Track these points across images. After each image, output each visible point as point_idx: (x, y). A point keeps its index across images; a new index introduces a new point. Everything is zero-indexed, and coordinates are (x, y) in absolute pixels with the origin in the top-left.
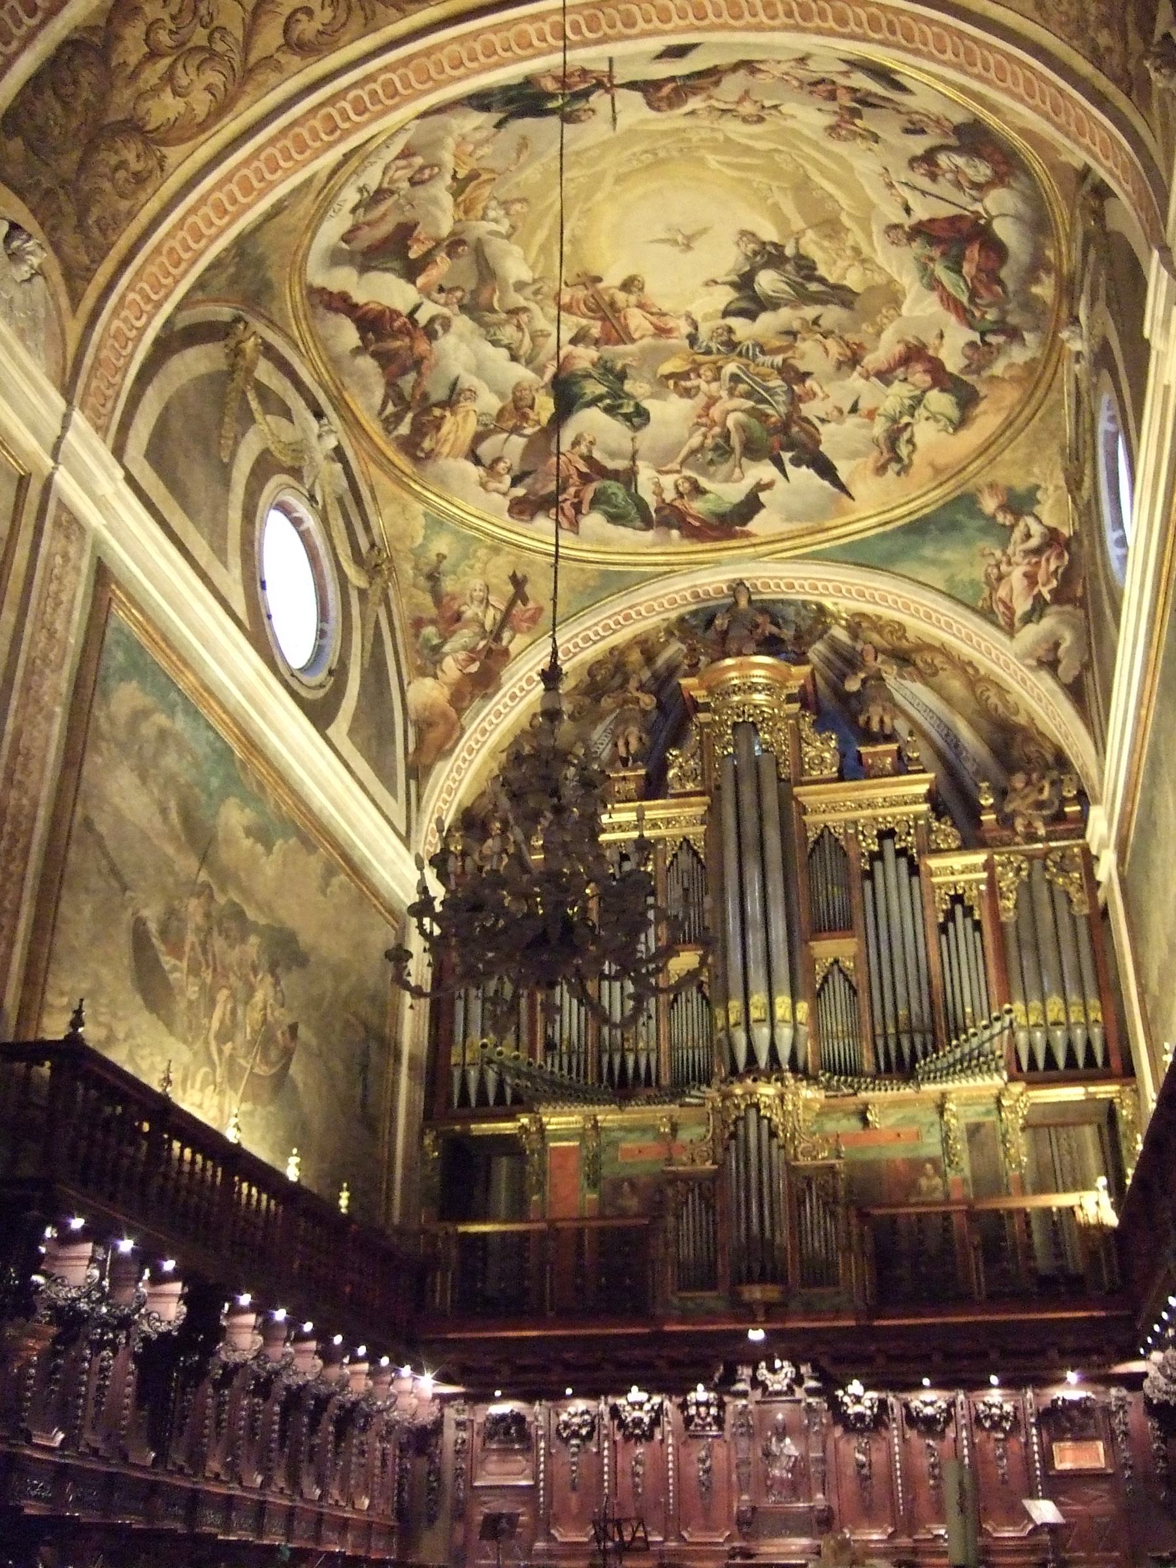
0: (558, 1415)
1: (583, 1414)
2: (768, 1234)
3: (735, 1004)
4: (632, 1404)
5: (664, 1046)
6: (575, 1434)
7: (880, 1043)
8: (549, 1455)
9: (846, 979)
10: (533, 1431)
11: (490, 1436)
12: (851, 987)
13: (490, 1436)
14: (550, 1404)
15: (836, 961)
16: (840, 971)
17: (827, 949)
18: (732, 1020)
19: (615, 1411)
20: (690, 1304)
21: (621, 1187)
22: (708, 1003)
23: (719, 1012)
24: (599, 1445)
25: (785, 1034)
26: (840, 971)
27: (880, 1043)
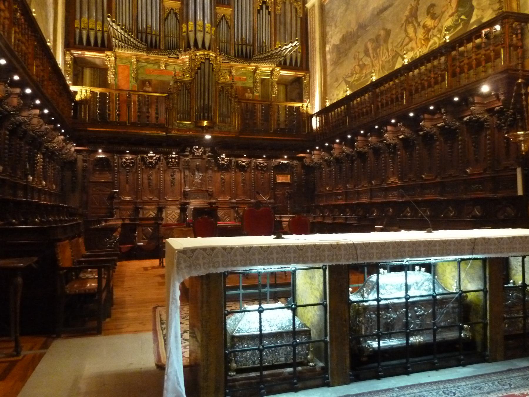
0: (122, 159)
1: (131, 159)
2: (210, 104)
3: (191, 23)
4: (149, 157)
5: (162, 35)
6: (128, 166)
7: (236, 46)
8: (118, 172)
9: (227, 22)
10: (112, 164)
11: (96, 165)
12: (228, 26)
13: (96, 165)
14: (119, 155)
15: (224, 16)
16: (225, 18)
17: (222, 10)
18: (190, 28)
19: (143, 159)
20: (181, 125)
21: (145, 83)
22: (179, 22)
23: (184, 26)
24: (136, 169)
25: (208, 37)
26: (225, 18)
27: (236, 46)
